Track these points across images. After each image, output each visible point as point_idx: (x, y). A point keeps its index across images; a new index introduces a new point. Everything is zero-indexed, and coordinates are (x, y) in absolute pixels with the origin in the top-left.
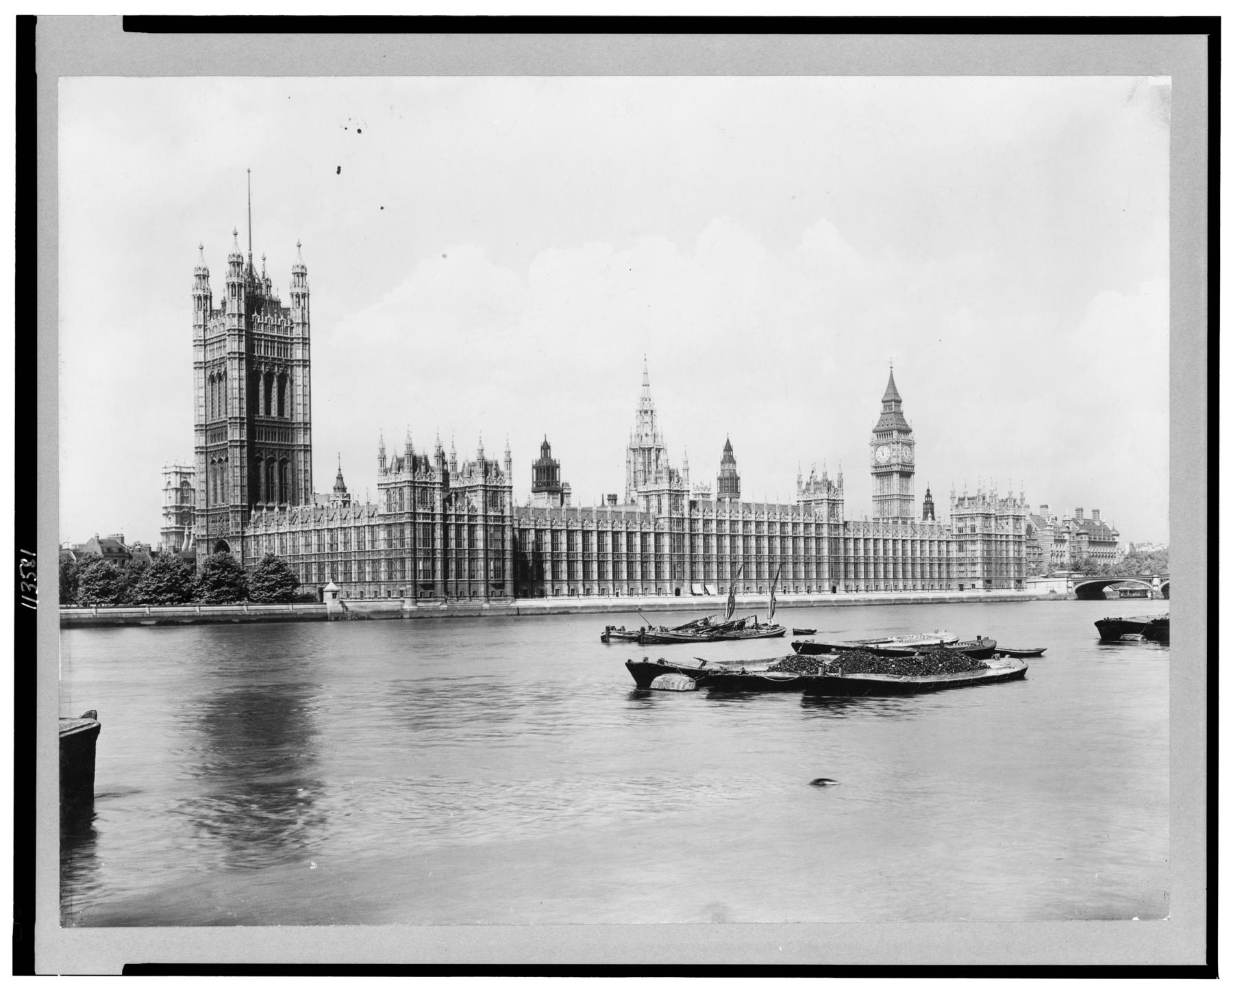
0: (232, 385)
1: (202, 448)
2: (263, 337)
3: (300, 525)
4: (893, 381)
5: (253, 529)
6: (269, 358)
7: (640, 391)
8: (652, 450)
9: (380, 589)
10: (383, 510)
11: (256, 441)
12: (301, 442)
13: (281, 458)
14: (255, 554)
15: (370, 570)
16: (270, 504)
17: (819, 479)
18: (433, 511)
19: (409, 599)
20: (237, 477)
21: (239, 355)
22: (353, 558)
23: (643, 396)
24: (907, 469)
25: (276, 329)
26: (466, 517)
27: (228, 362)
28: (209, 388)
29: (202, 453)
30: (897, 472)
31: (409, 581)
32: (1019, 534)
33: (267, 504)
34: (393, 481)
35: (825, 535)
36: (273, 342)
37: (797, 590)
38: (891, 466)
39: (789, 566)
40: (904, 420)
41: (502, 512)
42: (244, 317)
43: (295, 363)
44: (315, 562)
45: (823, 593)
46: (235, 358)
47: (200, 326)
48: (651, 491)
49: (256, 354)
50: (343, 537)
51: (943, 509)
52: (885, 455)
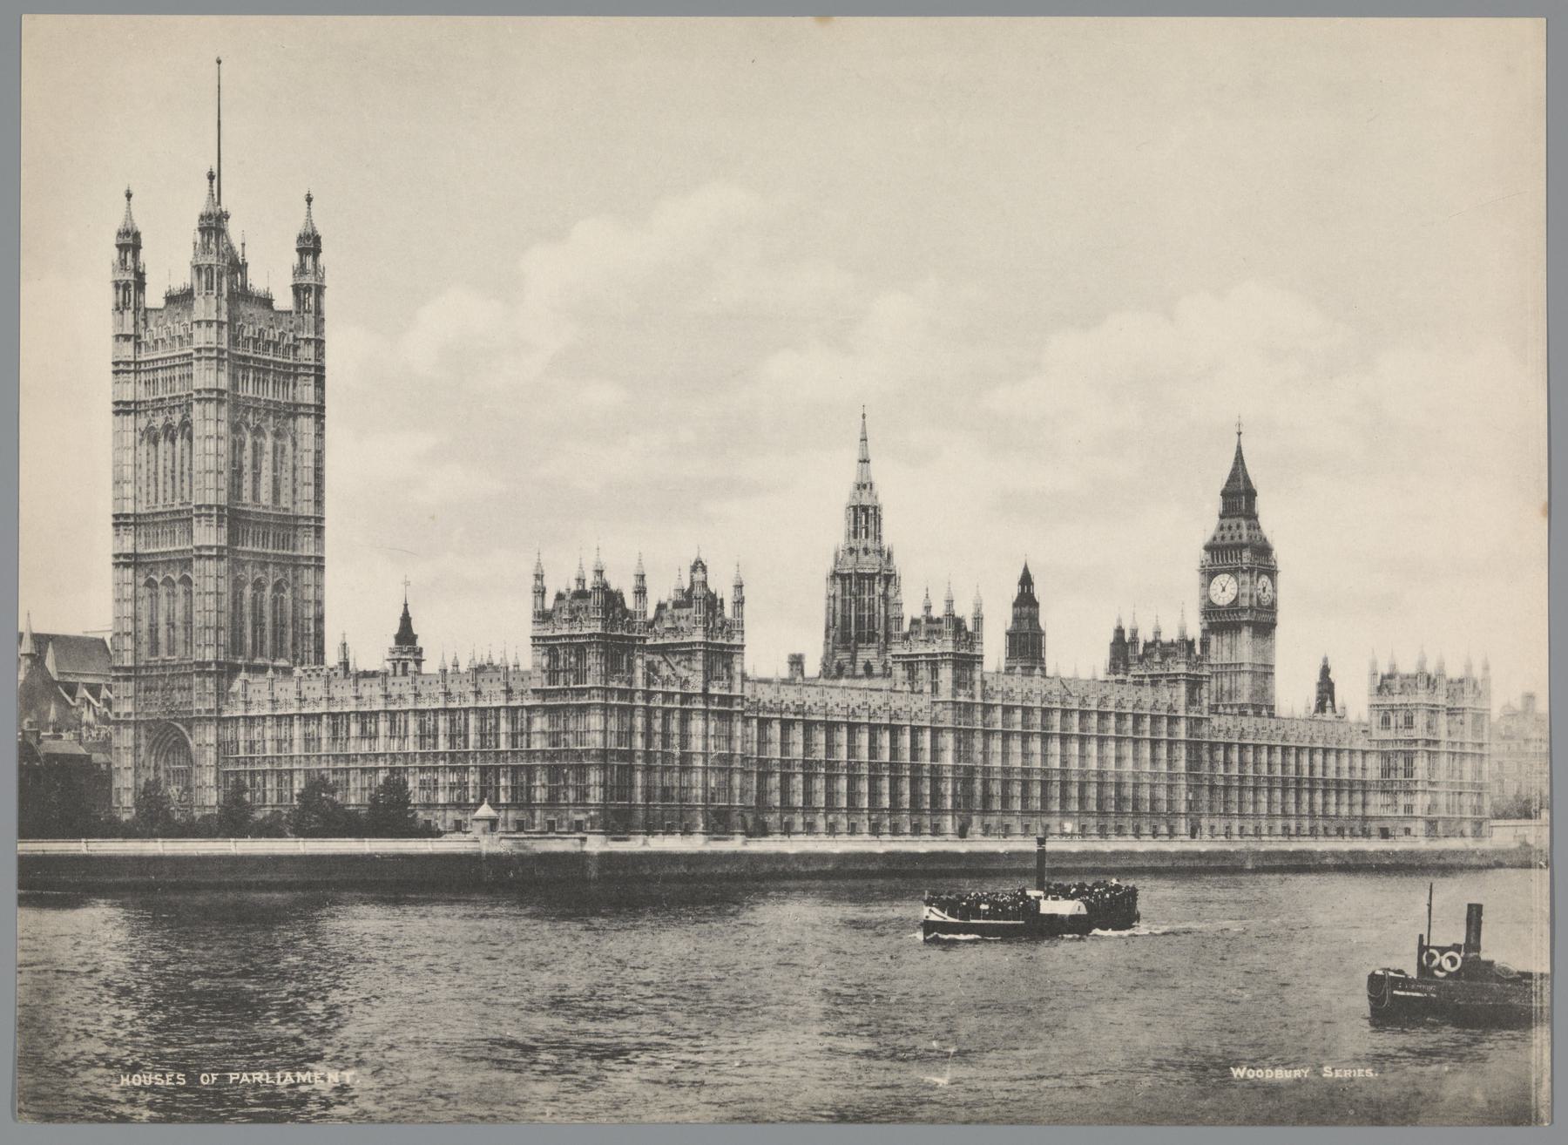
0: (205, 448)
1: (126, 556)
2: (252, 363)
3: (353, 702)
4: (1242, 458)
5: (241, 706)
6: (280, 403)
7: (851, 475)
8: (877, 578)
9: (533, 817)
10: (540, 682)
11: (239, 548)
12: (309, 550)
13: (275, 580)
14: (245, 750)
15: (509, 784)
16: (282, 663)
17: (938, 612)
18: (631, 685)
19: (702, 836)
20: (210, 611)
21: (218, 395)
22: (471, 763)
23: (859, 481)
24: (1263, 617)
25: (271, 350)
26: (678, 697)
27: (197, 407)
28: (143, 449)
29: (126, 565)
30: (1248, 623)
31: (597, 805)
32: (1480, 741)
33: (273, 661)
34: (565, 632)
35: (1183, 736)
36: (267, 372)
37: (1138, 831)
38: (1237, 612)
39: (841, 781)
40: (1259, 528)
41: (730, 688)
42: (226, 327)
43: (302, 410)
44: (385, 768)
45: (1159, 838)
46: (210, 400)
47: (127, 338)
48: (917, 656)
49: (240, 393)
50: (448, 725)
51: (1354, 698)
52: (1225, 590)
